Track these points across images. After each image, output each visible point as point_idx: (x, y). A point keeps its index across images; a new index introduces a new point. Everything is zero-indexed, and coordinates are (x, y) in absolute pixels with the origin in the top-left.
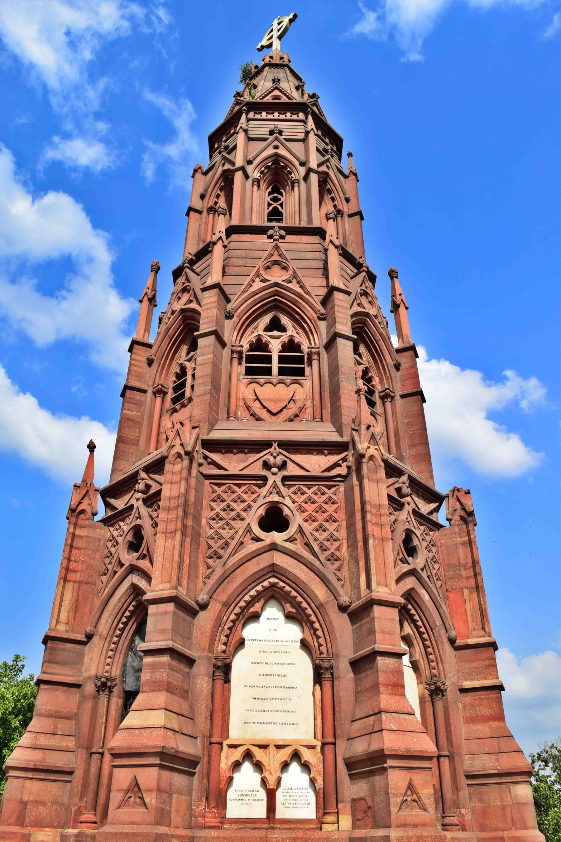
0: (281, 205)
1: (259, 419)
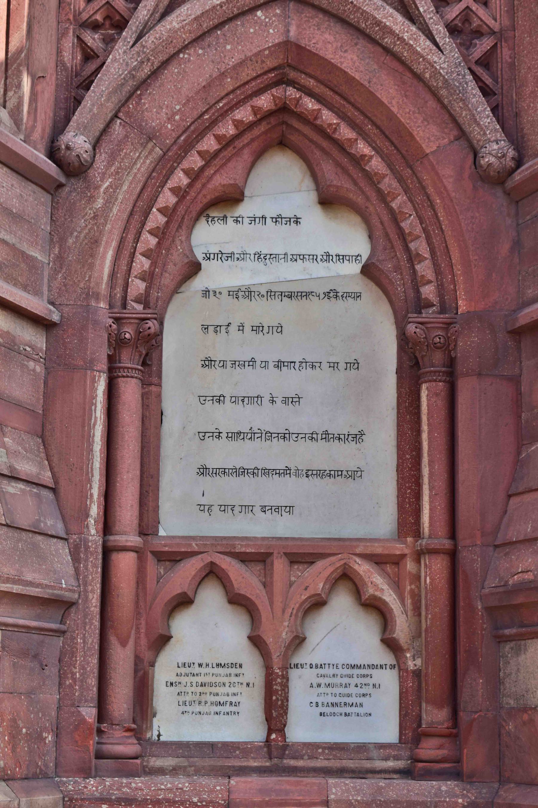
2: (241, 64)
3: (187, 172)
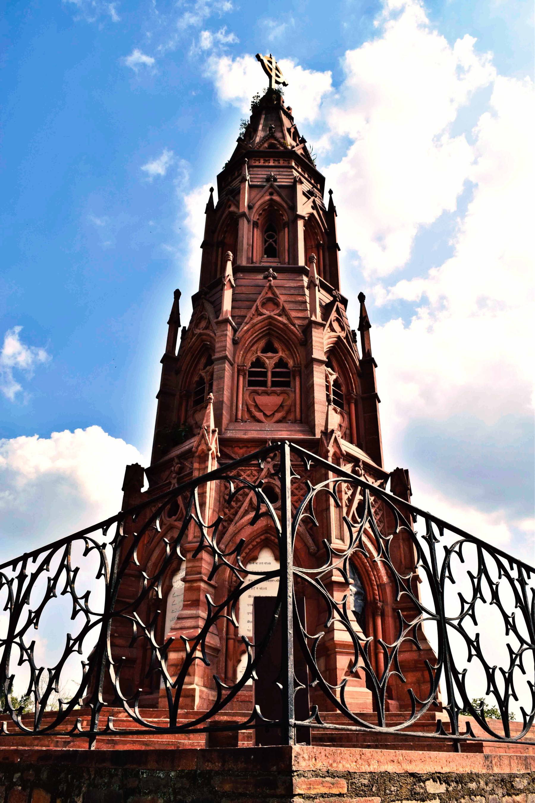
0: (275, 241)
1: (259, 421)
2: (258, 529)
3: (245, 553)
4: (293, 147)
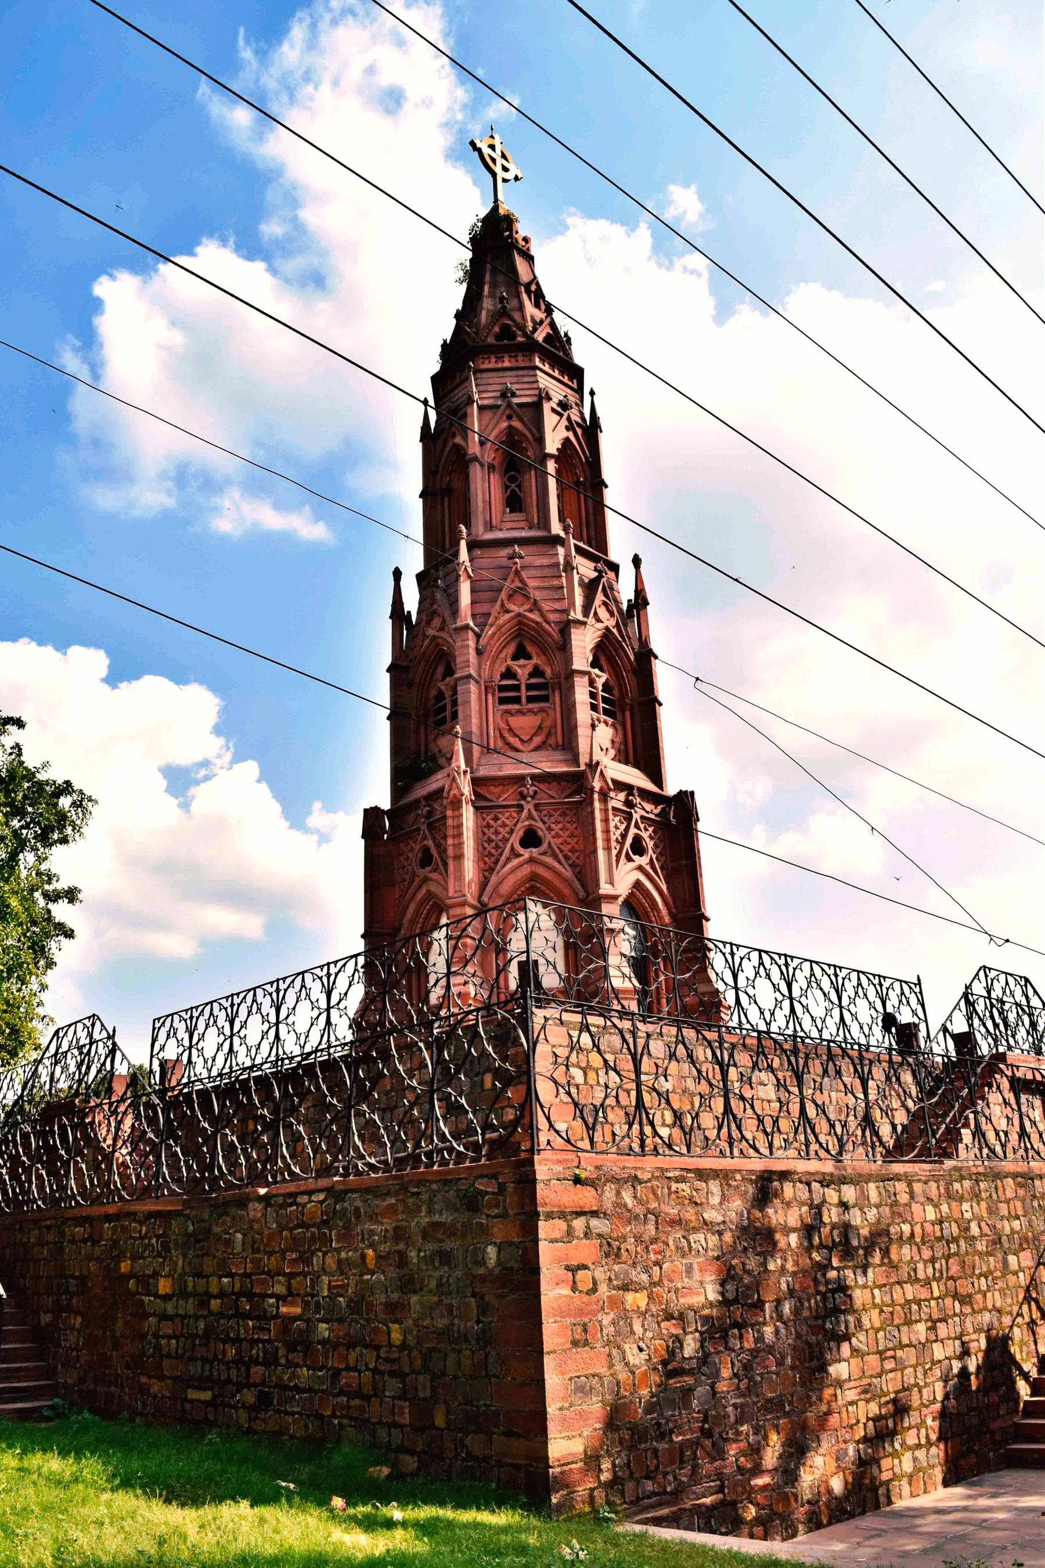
0: (519, 487)
4: (535, 330)
